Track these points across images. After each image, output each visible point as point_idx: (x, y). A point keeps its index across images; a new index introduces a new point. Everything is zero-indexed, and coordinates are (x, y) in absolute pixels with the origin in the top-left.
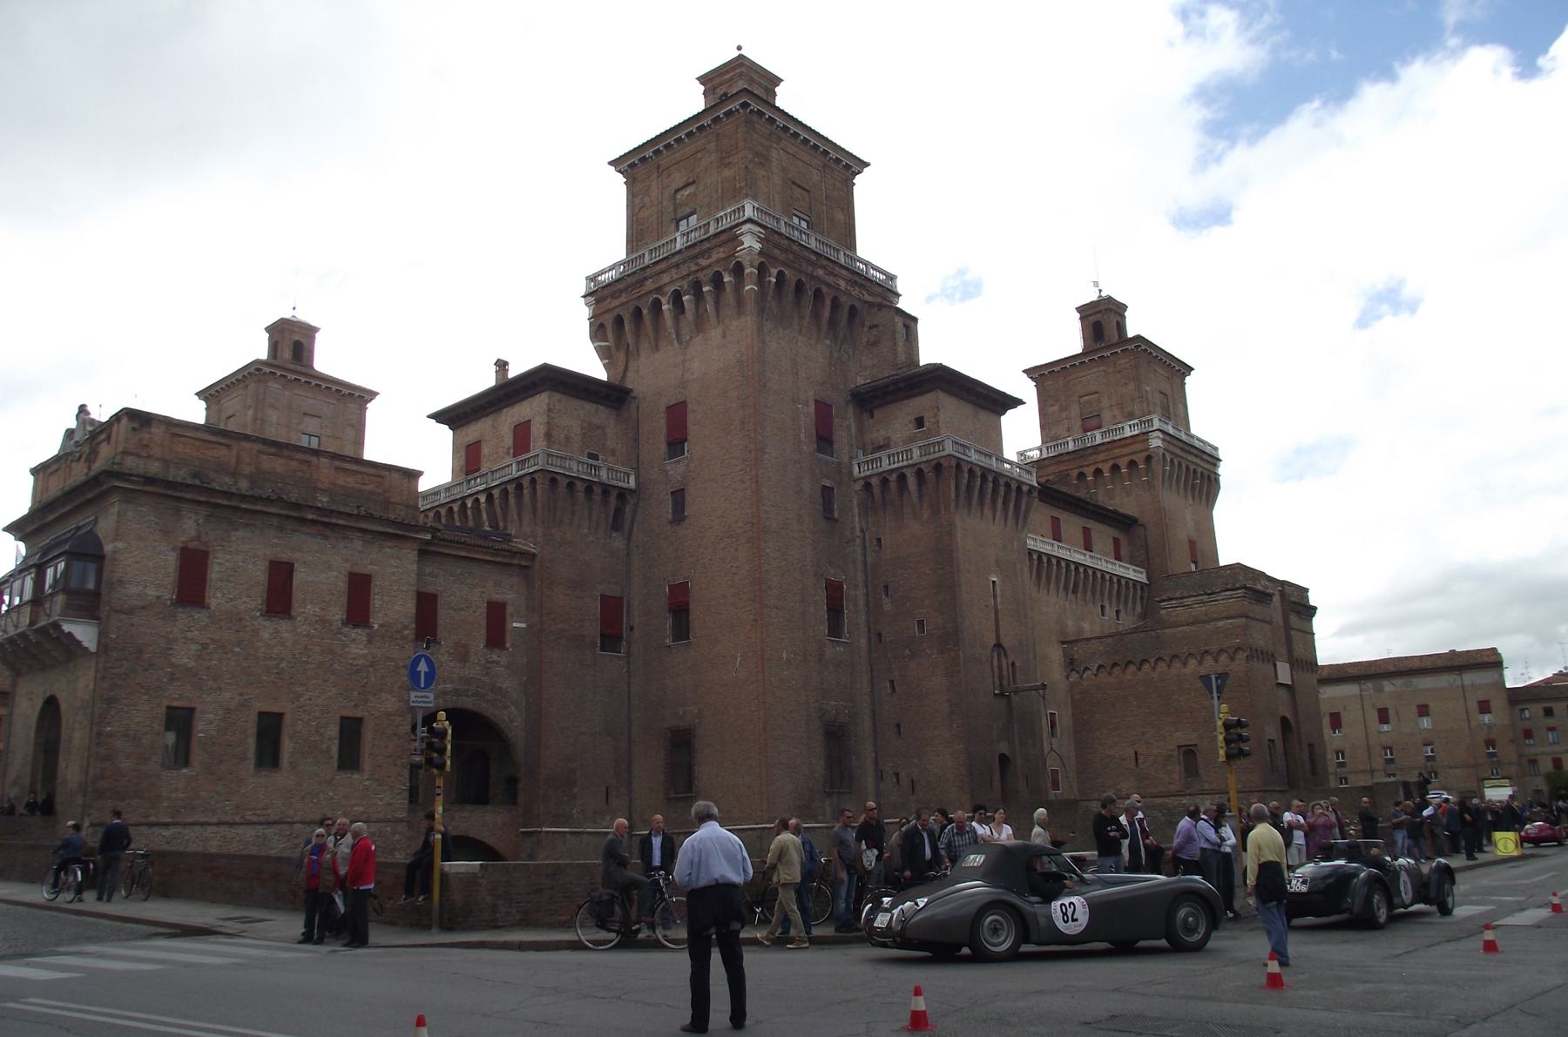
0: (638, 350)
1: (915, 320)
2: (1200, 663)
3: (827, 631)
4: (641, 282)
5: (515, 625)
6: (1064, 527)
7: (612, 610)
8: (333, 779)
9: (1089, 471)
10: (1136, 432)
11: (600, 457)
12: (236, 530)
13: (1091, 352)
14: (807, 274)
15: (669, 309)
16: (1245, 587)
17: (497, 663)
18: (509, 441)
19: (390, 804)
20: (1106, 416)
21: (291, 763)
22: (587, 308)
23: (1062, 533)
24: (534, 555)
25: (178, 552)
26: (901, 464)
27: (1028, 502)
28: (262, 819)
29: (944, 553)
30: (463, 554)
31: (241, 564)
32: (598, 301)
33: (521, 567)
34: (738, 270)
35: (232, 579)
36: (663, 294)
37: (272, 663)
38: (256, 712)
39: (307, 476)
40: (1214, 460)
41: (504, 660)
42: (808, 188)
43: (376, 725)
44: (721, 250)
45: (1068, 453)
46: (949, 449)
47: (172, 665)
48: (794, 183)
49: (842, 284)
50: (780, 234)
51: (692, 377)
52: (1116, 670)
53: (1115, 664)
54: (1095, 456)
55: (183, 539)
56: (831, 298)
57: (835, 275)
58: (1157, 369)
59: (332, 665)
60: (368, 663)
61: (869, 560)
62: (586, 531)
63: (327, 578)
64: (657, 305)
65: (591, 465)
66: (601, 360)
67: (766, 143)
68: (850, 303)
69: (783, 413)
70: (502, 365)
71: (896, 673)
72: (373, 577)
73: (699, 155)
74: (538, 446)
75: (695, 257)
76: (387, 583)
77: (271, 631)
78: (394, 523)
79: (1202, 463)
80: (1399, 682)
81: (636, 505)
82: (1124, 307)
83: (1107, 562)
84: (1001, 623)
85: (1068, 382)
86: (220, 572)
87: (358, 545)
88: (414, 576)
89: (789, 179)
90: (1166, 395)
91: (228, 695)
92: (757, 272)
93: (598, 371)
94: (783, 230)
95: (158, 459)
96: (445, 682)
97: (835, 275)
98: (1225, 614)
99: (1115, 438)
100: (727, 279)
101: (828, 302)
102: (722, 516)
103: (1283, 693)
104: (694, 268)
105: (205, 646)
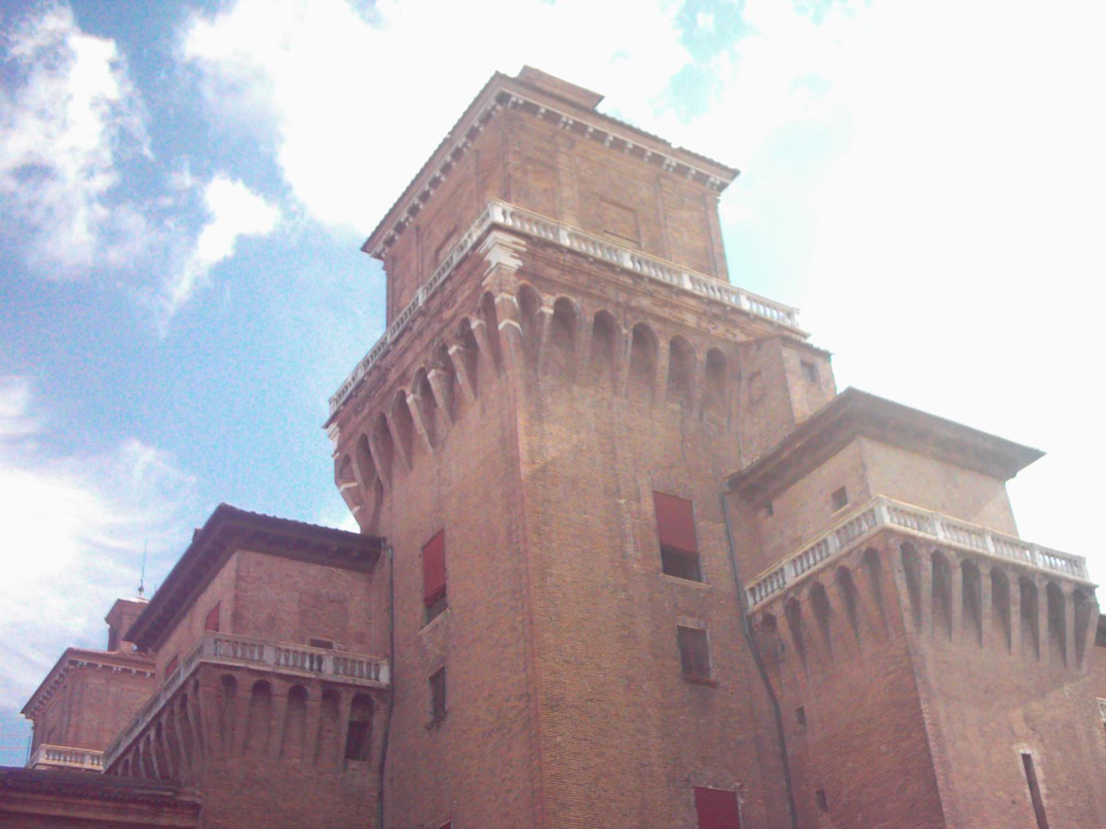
1: (826, 356)
4: (383, 378)
14: (617, 304)
15: (415, 400)
24: (196, 807)
26: (814, 569)
30: (60, 812)
32: (341, 426)
34: (488, 308)
44: (467, 286)
48: (603, 199)
49: (691, 320)
57: (674, 307)
65: (312, 656)
66: (351, 508)
68: (707, 346)
73: (460, 190)
97: (674, 307)
100: (475, 324)
101: (664, 345)
102: (491, 696)
104: (437, 326)
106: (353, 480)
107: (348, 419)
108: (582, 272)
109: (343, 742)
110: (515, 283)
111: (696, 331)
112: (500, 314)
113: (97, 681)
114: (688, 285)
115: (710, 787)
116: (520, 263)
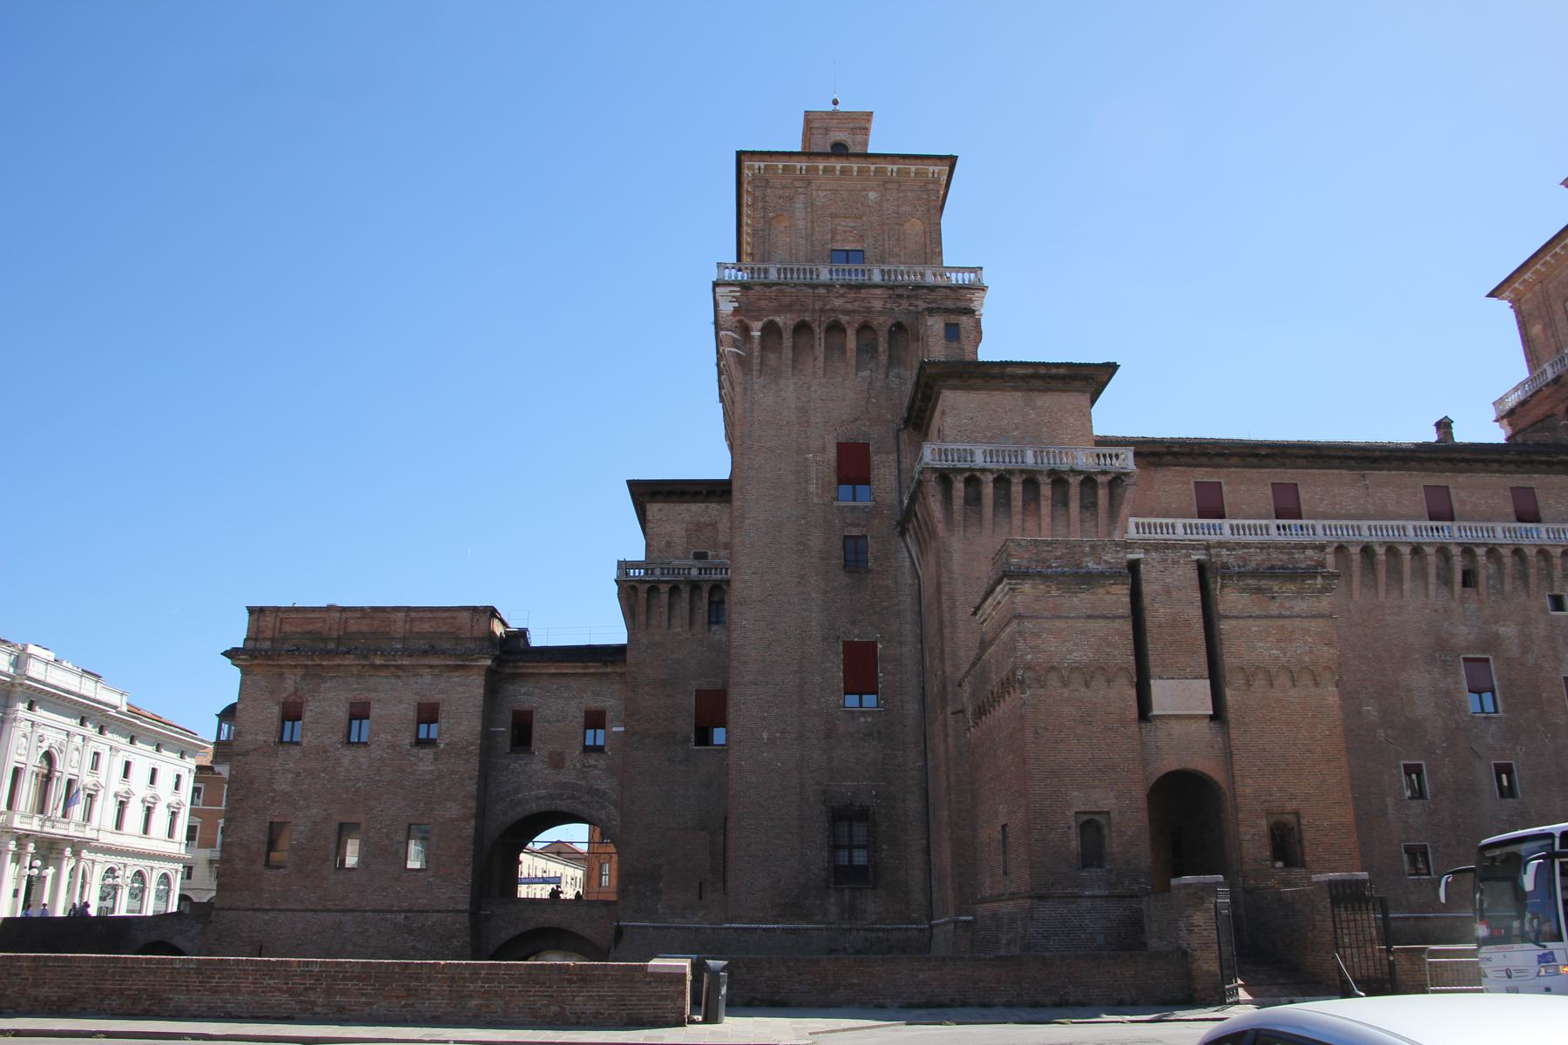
5: (614, 729)
11: (710, 554)
12: (326, 682)
17: (595, 767)
19: (451, 898)
25: (281, 705)
28: (339, 907)
30: (553, 671)
31: (327, 708)
35: (320, 720)
38: (337, 823)
41: (602, 763)
45: (1547, 385)
47: (274, 791)
49: (877, 305)
59: (401, 782)
62: (679, 629)
69: (780, 469)
72: (441, 706)
76: (453, 708)
77: (350, 758)
87: (428, 679)
91: (315, 811)
96: (538, 788)
114: (877, 278)
115: (856, 640)
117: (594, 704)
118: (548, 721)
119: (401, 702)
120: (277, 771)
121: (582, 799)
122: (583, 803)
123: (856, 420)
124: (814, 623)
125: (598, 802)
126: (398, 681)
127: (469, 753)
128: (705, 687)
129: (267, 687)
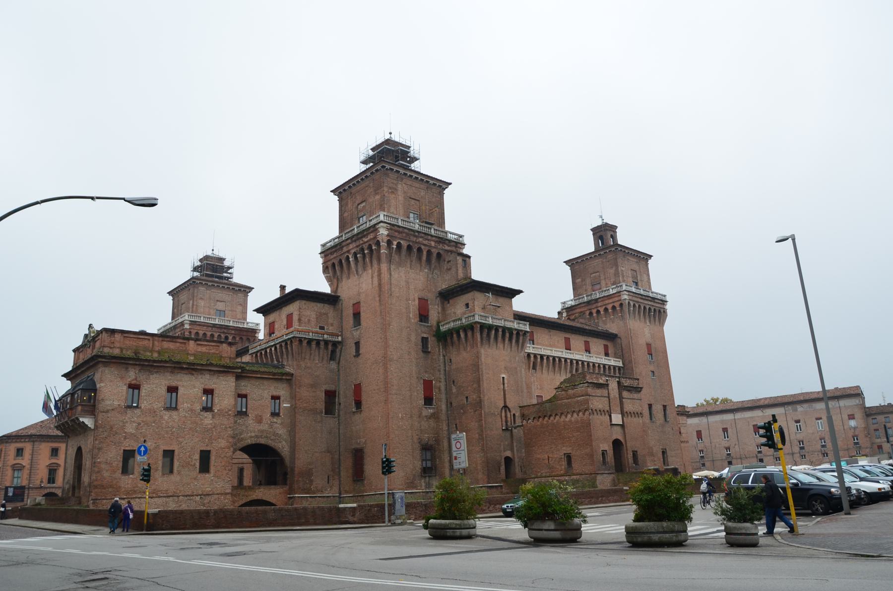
0: (342, 278)
1: (469, 257)
2: (572, 416)
3: (423, 403)
4: (342, 248)
5: (285, 405)
6: (572, 342)
7: (331, 395)
8: (197, 477)
9: (594, 311)
10: (615, 292)
11: (325, 327)
12: (153, 374)
13: (597, 251)
14: (413, 242)
15: (353, 260)
16: (587, 382)
17: (276, 422)
18: (285, 322)
19: (223, 487)
20: (603, 283)
21: (178, 471)
22: (321, 259)
23: (571, 345)
24: (293, 374)
27: (523, 339)
28: (165, 495)
29: (476, 367)
30: (259, 376)
32: (325, 256)
33: (286, 379)
35: (151, 395)
36: (350, 254)
37: (169, 429)
39: (184, 349)
40: (664, 302)
41: (279, 421)
42: (418, 199)
43: (216, 453)
44: (371, 234)
45: (584, 303)
46: (477, 319)
47: (125, 433)
48: (410, 198)
49: (433, 244)
50: (399, 226)
51: (363, 291)
52: (541, 420)
53: (540, 417)
54: (597, 304)
55: (129, 380)
56: (426, 250)
58: (630, 259)
60: (212, 427)
61: (447, 369)
62: (317, 361)
63: (194, 392)
64: (348, 258)
67: (395, 182)
68: (437, 251)
70: (283, 288)
71: (458, 421)
72: (215, 391)
73: (367, 188)
74: (296, 325)
75: (362, 237)
77: (168, 416)
78: (223, 366)
79: (655, 304)
80: (806, 405)
81: (341, 348)
82: (616, 227)
83: (596, 357)
84: (507, 396)
85: (585, 267)
86: (146, 393)
87: (207, 376)
88: (233, 388)
89: (408, 197)
90: (636, 271)
92: (386, 245)
93: (325, 288)
94: (400, 224)
95: (118, 348)
97: (428, 240)
98: (581, 394)
99: (605, 295)
100: (374, 248)
101: (425, 253)
102: (373, 354)
103: (619, 429)
104: (361, 242)
105: (139, 424)
106: (329, 273)
107: (328, 255)
108: (404, 233)
109: (329, 356)
110: (386, 239)
111: (434, 248)
112: (381, 248)
113: (203, 289)
116: (388, 232)
117: (275, 394)
118: (254, 400)
119: (195, 387)
120: (127, 422)
121: (271, 438)
122: (271, 440)
123: (424, 289)
124: (414, 371)
125: (278, 439)
126: (193, 376)
127: (229, 415)
128: (328, 389)
129: (118, 375)
